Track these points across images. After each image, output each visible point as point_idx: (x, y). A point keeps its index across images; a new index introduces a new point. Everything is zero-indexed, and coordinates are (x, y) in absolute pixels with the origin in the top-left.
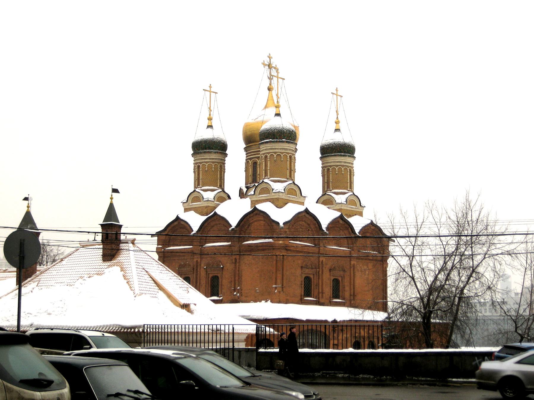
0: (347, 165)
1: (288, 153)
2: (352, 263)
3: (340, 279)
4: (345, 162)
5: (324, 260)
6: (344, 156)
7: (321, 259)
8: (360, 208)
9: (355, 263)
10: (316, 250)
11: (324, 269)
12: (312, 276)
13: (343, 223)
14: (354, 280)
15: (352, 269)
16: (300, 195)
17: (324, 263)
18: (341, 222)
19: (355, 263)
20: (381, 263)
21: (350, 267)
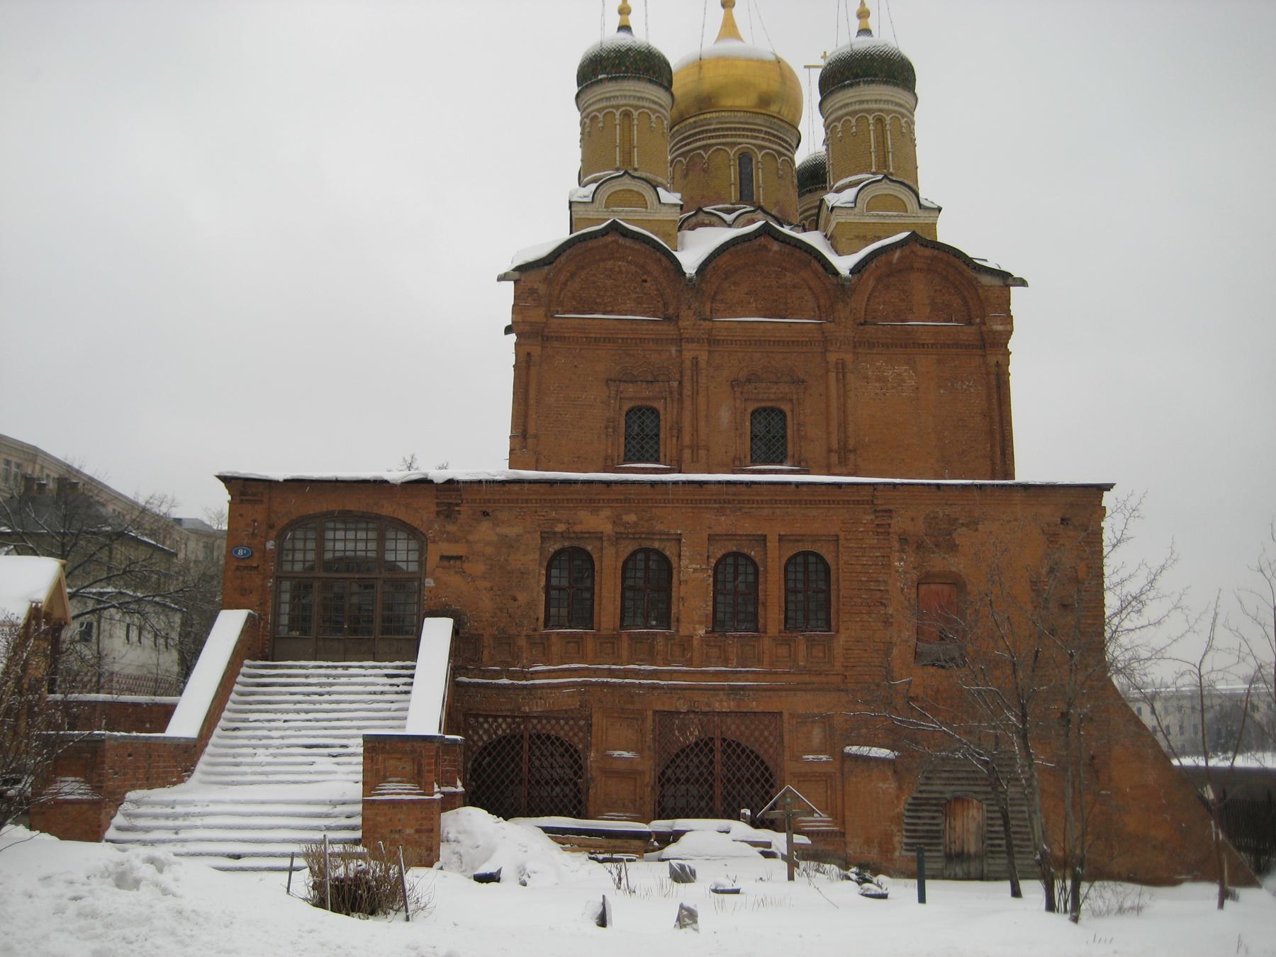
0: (882, 106)
1: (618, 107)
2: (832, 358)
3: (786, 407)
4: (862, 102)
5: (703, 357)
6: (851, 85)
7: (688, 355)
8: (920, 213)
9: (849, 358)
10: (668, 330)
11: (703, 380)
12: (659, 405)
13: (788, 249)
14: (844, 411)
15: (832, 376)
16: (656, 202)
17: (703, 364)
18: (776, 247)
19: (849, 358)
20: (981, 352)
21: (828, 371)
